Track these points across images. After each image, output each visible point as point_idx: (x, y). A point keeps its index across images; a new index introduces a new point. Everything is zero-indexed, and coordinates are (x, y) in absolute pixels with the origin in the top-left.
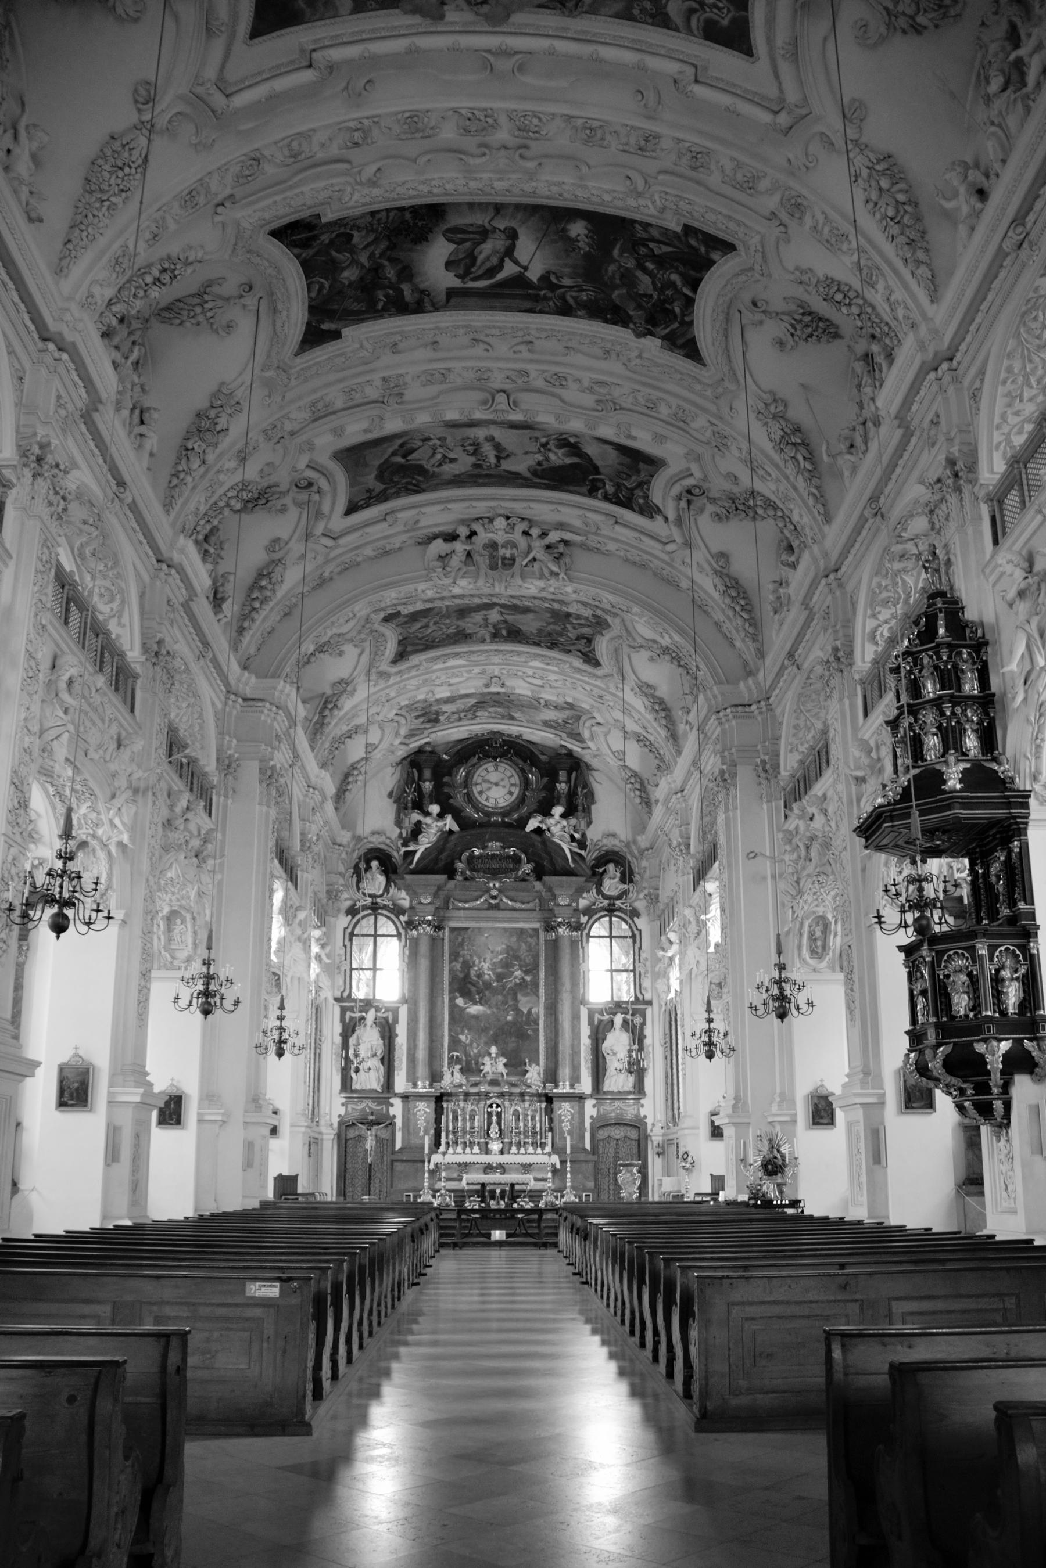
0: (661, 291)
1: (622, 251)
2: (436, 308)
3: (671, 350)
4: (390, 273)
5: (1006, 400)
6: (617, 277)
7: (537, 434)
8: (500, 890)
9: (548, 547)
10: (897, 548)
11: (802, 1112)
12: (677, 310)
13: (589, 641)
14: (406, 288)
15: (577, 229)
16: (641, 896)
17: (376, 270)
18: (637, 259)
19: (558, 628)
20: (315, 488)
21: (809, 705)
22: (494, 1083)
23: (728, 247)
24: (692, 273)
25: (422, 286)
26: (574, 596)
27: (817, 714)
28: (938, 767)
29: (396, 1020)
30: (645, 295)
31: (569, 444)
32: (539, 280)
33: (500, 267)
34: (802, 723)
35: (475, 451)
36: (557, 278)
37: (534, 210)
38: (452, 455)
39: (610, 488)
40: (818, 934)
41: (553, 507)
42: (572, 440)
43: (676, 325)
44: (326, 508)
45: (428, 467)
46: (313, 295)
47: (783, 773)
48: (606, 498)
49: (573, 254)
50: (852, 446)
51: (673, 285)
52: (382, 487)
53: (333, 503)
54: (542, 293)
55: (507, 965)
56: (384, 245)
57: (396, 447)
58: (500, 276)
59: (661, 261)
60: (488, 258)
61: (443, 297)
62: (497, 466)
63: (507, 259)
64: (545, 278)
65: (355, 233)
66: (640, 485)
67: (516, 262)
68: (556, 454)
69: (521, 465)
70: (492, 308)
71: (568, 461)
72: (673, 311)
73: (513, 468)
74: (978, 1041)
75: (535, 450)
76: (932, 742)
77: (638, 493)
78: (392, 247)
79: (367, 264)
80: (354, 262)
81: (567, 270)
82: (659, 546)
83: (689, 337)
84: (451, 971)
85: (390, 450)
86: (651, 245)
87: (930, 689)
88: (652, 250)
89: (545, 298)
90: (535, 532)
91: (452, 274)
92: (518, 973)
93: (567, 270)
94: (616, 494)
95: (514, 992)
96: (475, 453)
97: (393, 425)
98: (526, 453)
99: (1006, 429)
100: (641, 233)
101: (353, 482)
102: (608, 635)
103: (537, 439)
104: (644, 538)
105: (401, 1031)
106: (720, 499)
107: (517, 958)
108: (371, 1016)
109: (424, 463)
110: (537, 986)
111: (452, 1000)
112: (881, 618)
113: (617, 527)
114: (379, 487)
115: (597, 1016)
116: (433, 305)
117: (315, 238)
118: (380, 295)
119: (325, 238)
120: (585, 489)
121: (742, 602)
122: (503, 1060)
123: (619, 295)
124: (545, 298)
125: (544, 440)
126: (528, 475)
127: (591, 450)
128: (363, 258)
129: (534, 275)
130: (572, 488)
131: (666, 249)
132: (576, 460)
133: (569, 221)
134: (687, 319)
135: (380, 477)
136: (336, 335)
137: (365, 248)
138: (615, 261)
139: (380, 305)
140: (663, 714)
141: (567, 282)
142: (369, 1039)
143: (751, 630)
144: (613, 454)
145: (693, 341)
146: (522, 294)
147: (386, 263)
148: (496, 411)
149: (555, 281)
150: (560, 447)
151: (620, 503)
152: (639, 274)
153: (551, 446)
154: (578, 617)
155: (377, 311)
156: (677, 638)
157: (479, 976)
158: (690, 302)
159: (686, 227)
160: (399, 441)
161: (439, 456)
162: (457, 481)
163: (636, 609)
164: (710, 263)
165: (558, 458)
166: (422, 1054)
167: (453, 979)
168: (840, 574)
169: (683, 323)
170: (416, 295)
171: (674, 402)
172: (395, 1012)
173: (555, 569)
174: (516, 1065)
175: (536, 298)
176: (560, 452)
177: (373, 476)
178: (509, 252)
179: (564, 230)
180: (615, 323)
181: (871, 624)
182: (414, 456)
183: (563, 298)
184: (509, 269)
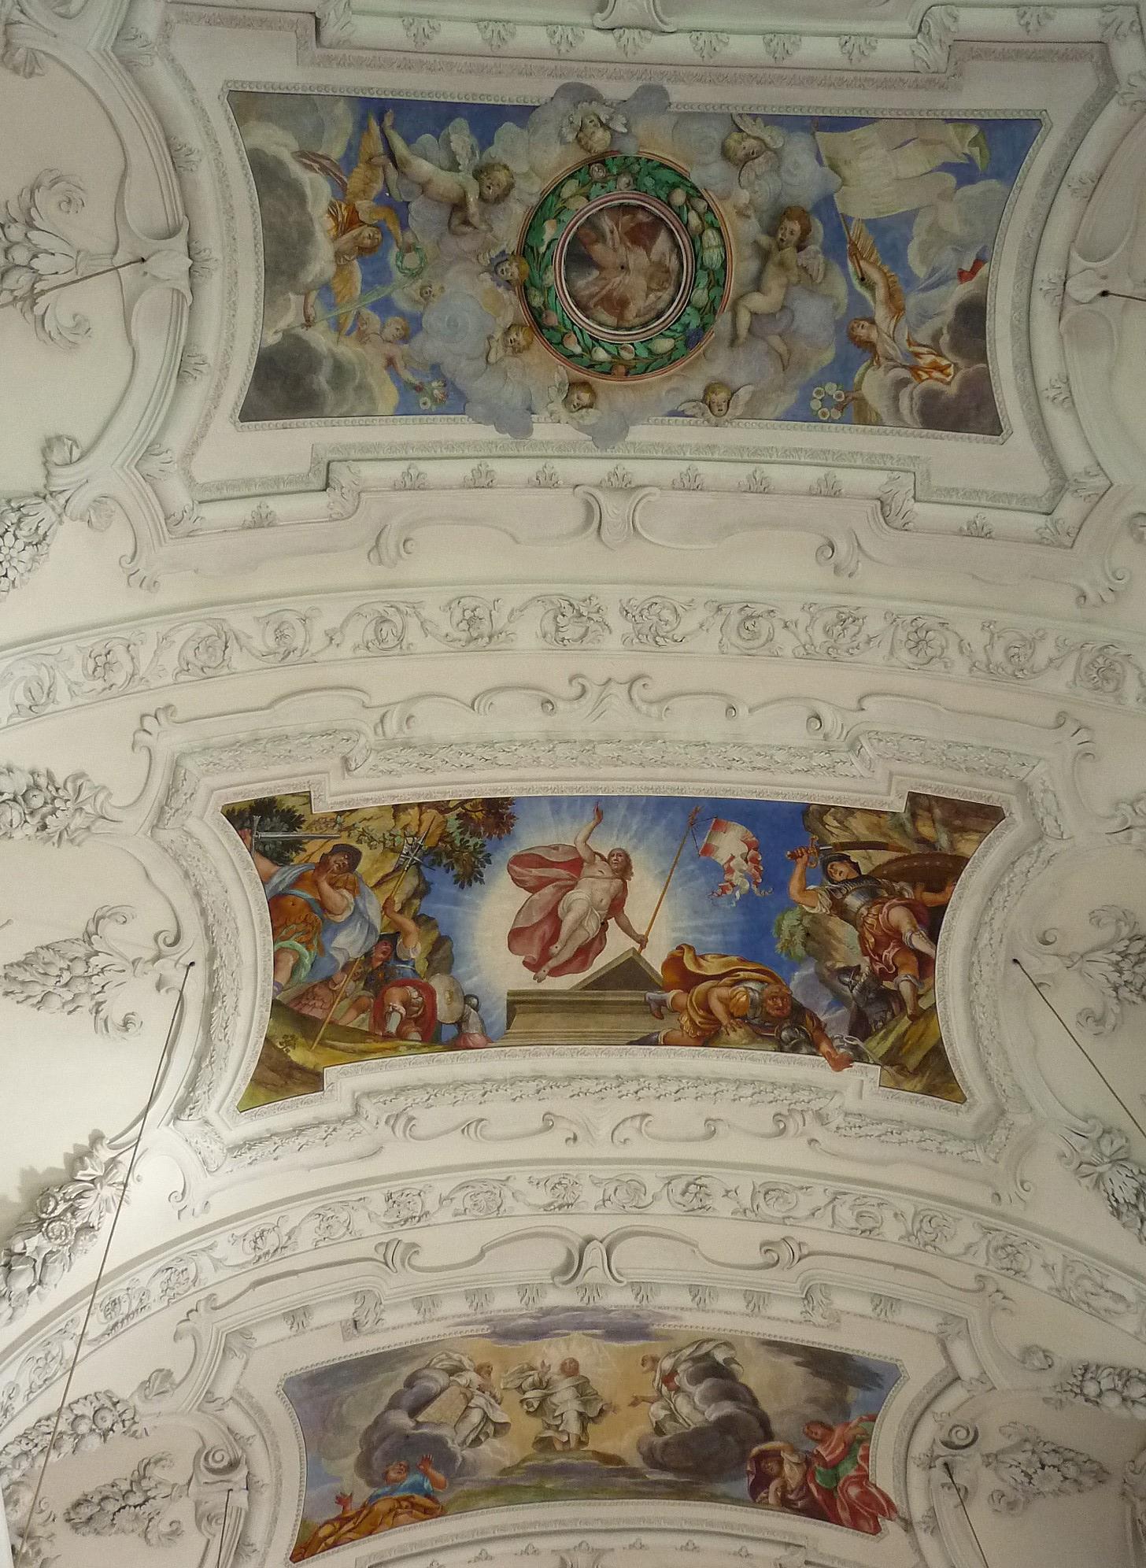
0: (874, 953)
1: (806, 880)
2: (489, 1041)
3: (898, 1086)
4: (415, 949)
6: (799, 938)
7: (657, 1348)
12: (905, 989)
14: (439, 983)
15: (731, 844)
17: (392, 938)
18: (831, 893)
20: (240, 1476)
23: (987, 816)
24: (928, 897)
25: (468, 985)
30: (846, 971)
31: (716, 1372)
32: (665, 966)
33: (600, 939)
35: (543, 1400)
36: (696, 959)
37: (661, 806)
38: (499, 1416)
39: (792, 1473)
42: (720, 1356)
43: (905, 1023)
44: (258, 1534)
45: (453, 1446)
46: (283, 977)
48: (785, 1504)
49: (723, 901)
51: (894, 935)
52: (369, 1491)
53: (275, 1520)
54: (670, 996)
56: (410, 883)
57: (399, 1385)
58: (601, 962)
59: (872, 886)
60: (580, 923)
61: (501, 1012)
62: (581, 1443)
63: (612, 922)
64: (674, 962)
65: (363, 848)
67: (627, 929)
68: (689, 1396)
69: (621, 1438)
70: (584, 1039)
71: (713, 1413)
72: (897, 994)
73: (608, 1447)
75: (651, 1393)
77: (848, 1470)
78: (422, 891)
79: (378, 924)
80: (358, 913)
81: (713, 939)
83: (930, 1042)
85: (389, 1392)
86: (855, 855)
88: (856, 866)
89: (676, 1010)
91: (520, 959)
93: (713, 939)
94: (804, 1485)
96: (540, 1410)
97: (398, 1328)
98: (635, 1403)
100: (836, 834)
101: (314, 1476)
103: (655, 1360)
106: (1003, 1451)
109: (445, 1432)
114: (362, 1492)
116: (484, 1031)
117: (296, 845)
118: (395, 998)
119: (315, 850)
120: (743, 1486)
123: (804, 979)
124: (676, 1010)
125: (667, 1364)
126: (636, 1461)
127: (754, 1375)
128: (373, 908)
129: (655, 958)
130: (721, 1488)
131: (881, 857)
132: (727, 1408)
133: (717, 827)
134: (924, 1004)
135: (364, 1465)
136: (313, 1081)
137: (379, 884)
138: (795, 904)
139: (393, 1026)
141: (712, 967)
144: (795, 1373)
145: (938, 1050)
146: (637, 1001)
147: (410, 925)
148: (584, 1287)
149: (691, 967)
150: (696, 1379)
152: (838, 926)
153: (681, 1379)
155: (387, 1037)
158: (925, 965)
159: (913, 798)
160: (406, 1371)
161: (475, 1417)
162: (507, 1488)
164: (958, 863)
165: (696, 1408)
169: (914, 1018)
170: (458, 1006)
171: (907, 1206)
175: (659, 1010)
176: (698, 1391)
177: (351, 1460)
178: (616, 907)
179: (708, 850)
180: (795, 1049)
182: (428, 1414)
183: (705, 1006)
184: (617, 946)
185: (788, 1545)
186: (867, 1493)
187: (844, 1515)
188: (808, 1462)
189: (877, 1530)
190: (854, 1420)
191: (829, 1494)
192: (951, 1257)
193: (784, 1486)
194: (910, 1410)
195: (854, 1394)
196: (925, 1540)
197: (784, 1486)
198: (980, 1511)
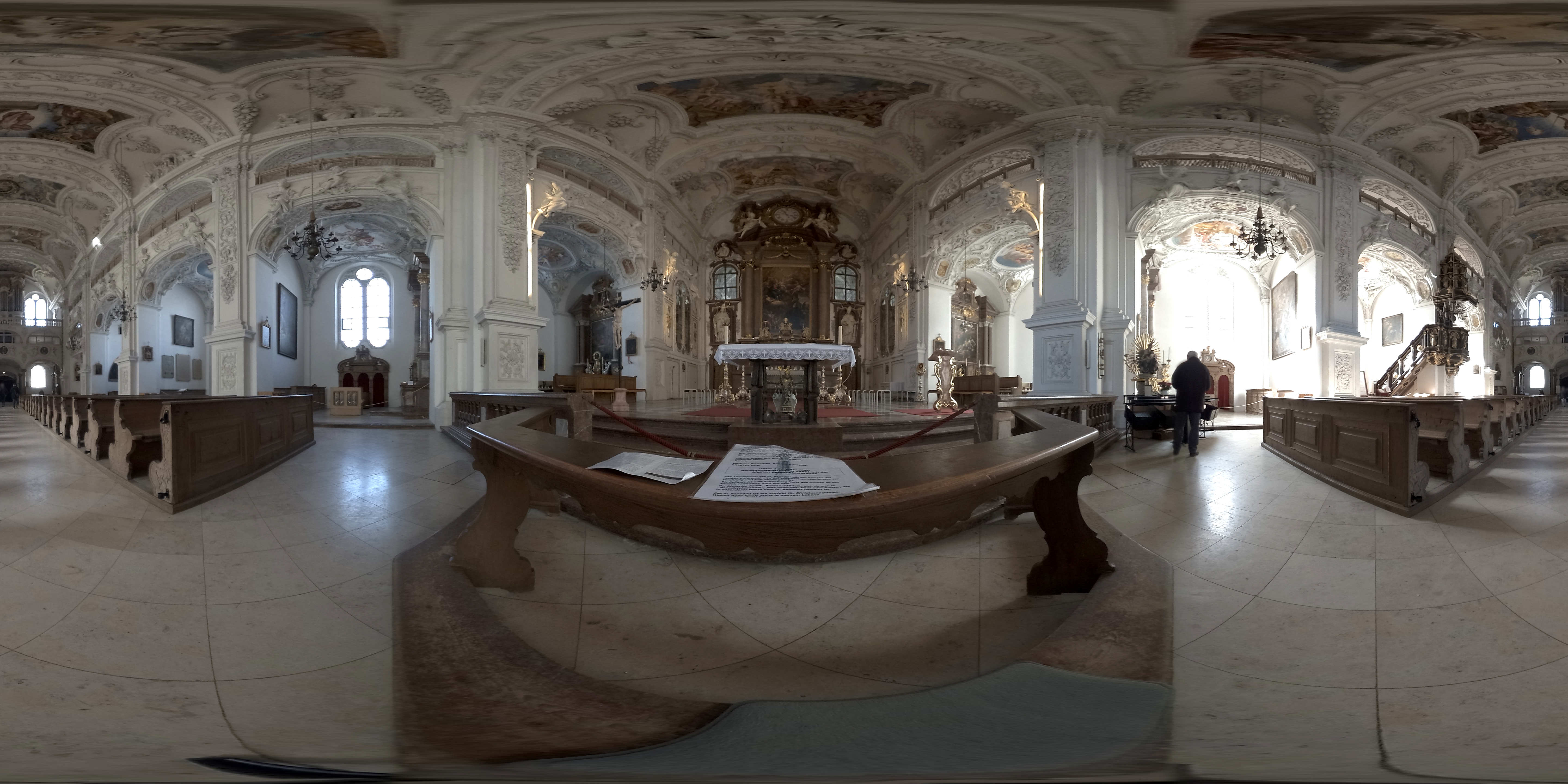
8: (789, 250)
22: (785, 335)
29: (736, 309)
55: (793, 283)
84: (764, 285)
92: (799, 286)
95: (796, 295)
105: (739, 313)
107: (798, 280)
108: (724, 307)
110: (808, 291)
111: (764, 298)
115: (838, 308)
122: (790, 325)
142: (722, 317)
157: (778, 287)
166: (748, 322)
167: (764, 290)
172: (736, 305)
174: (797, 326)
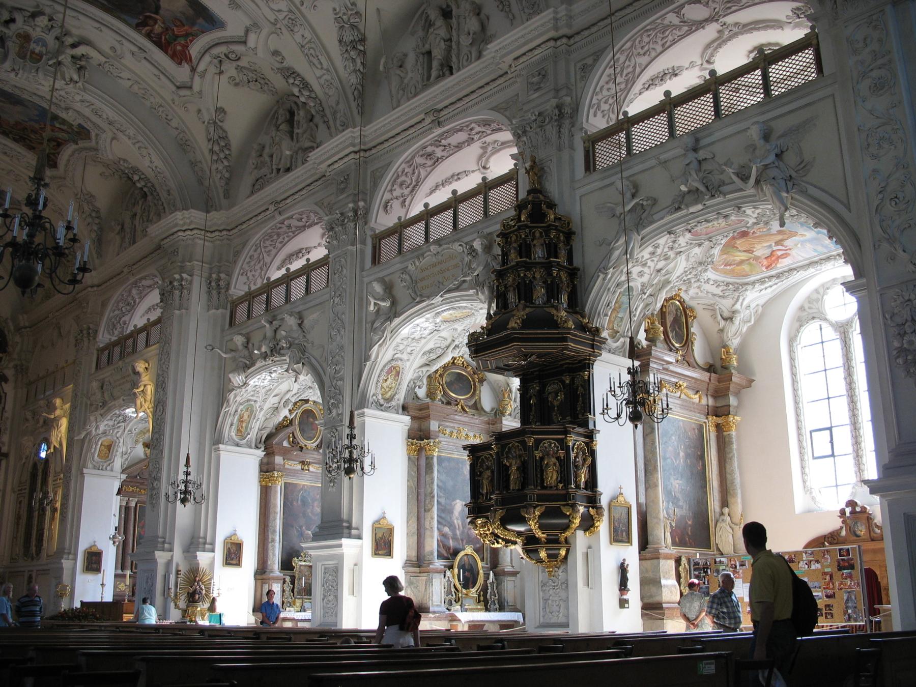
5: (607, 79)
9: (73, 57)
10: (429, 149)
11: (219, 554)
13: (59, 145)
16: (11, 365)
19: (37, 126)
21: (268, 243)
26: (79, 104)
27: (270, 251)
28: (547, 310)
34: (256, 256)
39: (158, 28)
40: (245, 417)
41: (97, 25)
47: (232, 291)
48: (148, 36)
50: (401, 66)
66: (187, 35)
74: (564, 505)
76: (540, 293)
82: (174, 88)
87: (539, 253)
90: (69, 40)
99: (600, 97)
102: (82, 144)
104: (162, 77)
112: (395, 194)
113: (144, 61)
121: (227, 152)
140: (97, 221)
143: (227, 175)
151: (158, 44)
154: (64, 122)
156: (158, 163)
163: (131, 132)
168: (368, 154)
173: (76, 77)
181: (387, 196)
185: (140, 48)
186: (184, 51)
187: (170, 52)
188: (167, 29)
189: (180, 63)
190: (195, 28)
191: (168, 43)
192: (272, 9)
193: (151, 31)
194: (219, 38)
195: (201, 21)
196: (197, 79)
197: (151, 31)
198: (224, 78)
